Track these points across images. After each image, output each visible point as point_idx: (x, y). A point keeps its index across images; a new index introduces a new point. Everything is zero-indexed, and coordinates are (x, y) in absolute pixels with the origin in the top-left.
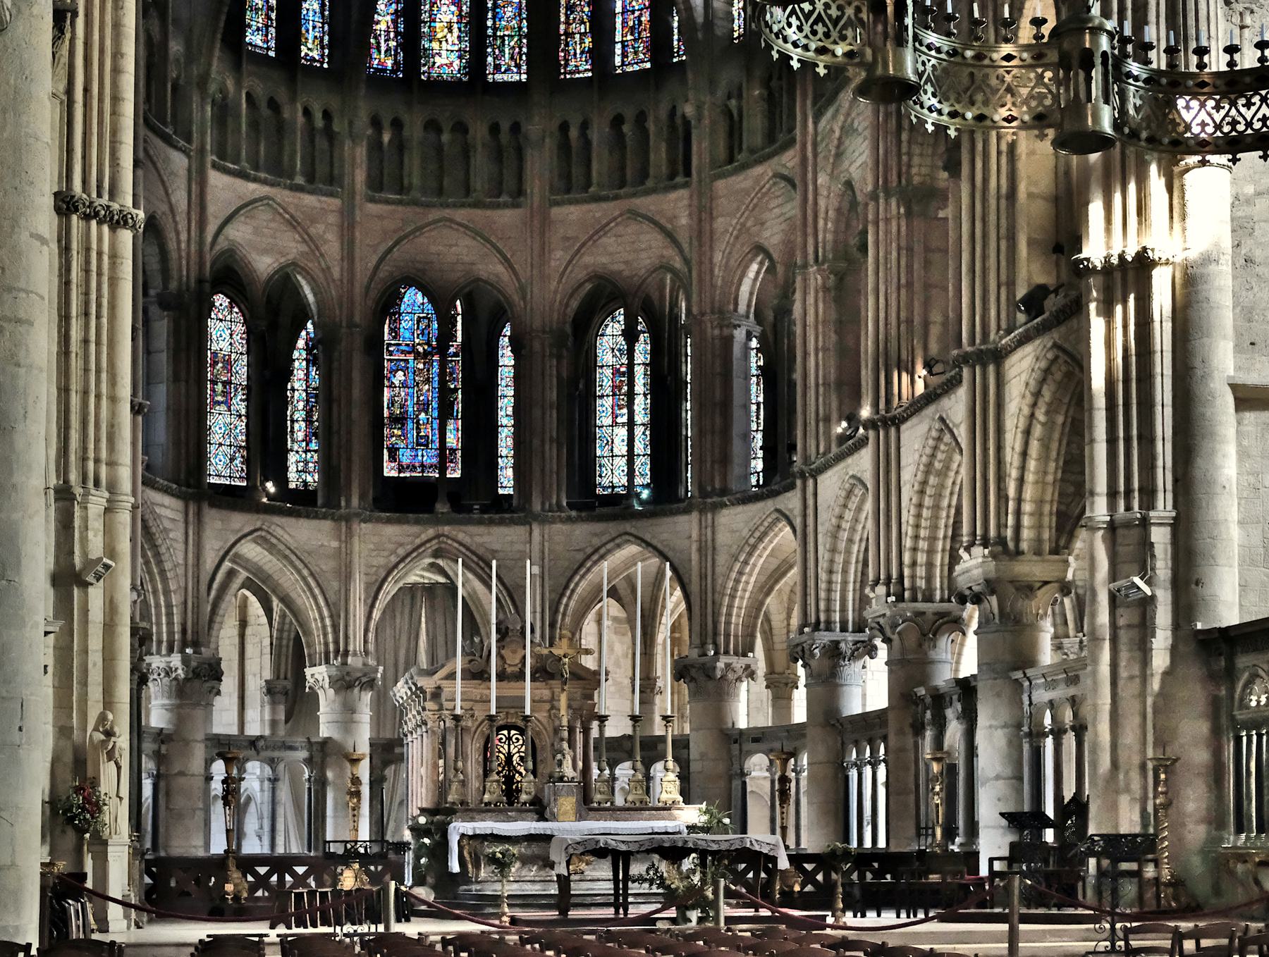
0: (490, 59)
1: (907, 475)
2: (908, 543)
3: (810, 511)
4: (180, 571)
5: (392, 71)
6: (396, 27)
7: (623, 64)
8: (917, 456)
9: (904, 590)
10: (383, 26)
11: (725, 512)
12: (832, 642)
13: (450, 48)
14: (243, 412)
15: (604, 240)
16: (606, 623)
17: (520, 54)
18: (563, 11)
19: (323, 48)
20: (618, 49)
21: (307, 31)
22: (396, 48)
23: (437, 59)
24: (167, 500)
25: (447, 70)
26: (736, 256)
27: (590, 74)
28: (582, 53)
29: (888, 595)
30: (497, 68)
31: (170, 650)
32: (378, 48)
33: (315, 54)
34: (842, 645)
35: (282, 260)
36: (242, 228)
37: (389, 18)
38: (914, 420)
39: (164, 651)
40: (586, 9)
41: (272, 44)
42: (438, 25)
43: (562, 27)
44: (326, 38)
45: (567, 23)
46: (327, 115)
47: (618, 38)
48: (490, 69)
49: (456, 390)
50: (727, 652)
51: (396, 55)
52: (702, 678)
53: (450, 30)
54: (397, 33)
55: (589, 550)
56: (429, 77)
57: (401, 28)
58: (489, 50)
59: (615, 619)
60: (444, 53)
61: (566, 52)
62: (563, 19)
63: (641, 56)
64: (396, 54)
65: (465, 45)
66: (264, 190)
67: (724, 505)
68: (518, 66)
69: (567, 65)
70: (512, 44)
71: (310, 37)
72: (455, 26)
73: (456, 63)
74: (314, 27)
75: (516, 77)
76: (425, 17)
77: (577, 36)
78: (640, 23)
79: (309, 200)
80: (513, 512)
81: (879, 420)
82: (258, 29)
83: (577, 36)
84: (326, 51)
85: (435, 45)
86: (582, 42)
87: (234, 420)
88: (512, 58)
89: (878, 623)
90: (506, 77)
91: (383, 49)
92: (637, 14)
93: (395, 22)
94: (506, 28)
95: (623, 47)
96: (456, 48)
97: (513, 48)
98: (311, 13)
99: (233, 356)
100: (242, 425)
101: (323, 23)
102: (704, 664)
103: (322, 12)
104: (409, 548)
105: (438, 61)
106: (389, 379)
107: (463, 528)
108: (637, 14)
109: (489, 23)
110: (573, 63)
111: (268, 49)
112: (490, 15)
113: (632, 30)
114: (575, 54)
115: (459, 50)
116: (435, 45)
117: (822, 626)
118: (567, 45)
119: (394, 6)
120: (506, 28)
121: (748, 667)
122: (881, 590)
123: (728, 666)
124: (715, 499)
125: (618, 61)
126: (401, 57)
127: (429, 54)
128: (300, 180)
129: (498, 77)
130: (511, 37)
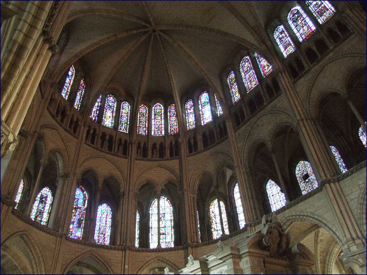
7: (154, 134)
19: (78, 107)
23: (106, 122)
28: (143, 131)
30: (121, 129)
35: (57, 147)
43: (138, 125)
44: (79, 106)
45: (139, 124)
47: (153, 129)
49: (83, 220)
54: (96, 113)
55: (145, 262)
60: (107, 121)
61: (139, 130)
62: (138, 123)
64: (95, 118)
77: (142, 128)
83: (142, 128)
84: (79, 109)
85: (106, 119)
86: (143, 129)
88: (125, 128)
90: (123, 131)
93: (97, 111)
105: (106, 123)
110: (140, 132)
113: (157, 128)
114: (141, 131)
116: (106, 119)
118: (139, 128)
126: (97, 118)
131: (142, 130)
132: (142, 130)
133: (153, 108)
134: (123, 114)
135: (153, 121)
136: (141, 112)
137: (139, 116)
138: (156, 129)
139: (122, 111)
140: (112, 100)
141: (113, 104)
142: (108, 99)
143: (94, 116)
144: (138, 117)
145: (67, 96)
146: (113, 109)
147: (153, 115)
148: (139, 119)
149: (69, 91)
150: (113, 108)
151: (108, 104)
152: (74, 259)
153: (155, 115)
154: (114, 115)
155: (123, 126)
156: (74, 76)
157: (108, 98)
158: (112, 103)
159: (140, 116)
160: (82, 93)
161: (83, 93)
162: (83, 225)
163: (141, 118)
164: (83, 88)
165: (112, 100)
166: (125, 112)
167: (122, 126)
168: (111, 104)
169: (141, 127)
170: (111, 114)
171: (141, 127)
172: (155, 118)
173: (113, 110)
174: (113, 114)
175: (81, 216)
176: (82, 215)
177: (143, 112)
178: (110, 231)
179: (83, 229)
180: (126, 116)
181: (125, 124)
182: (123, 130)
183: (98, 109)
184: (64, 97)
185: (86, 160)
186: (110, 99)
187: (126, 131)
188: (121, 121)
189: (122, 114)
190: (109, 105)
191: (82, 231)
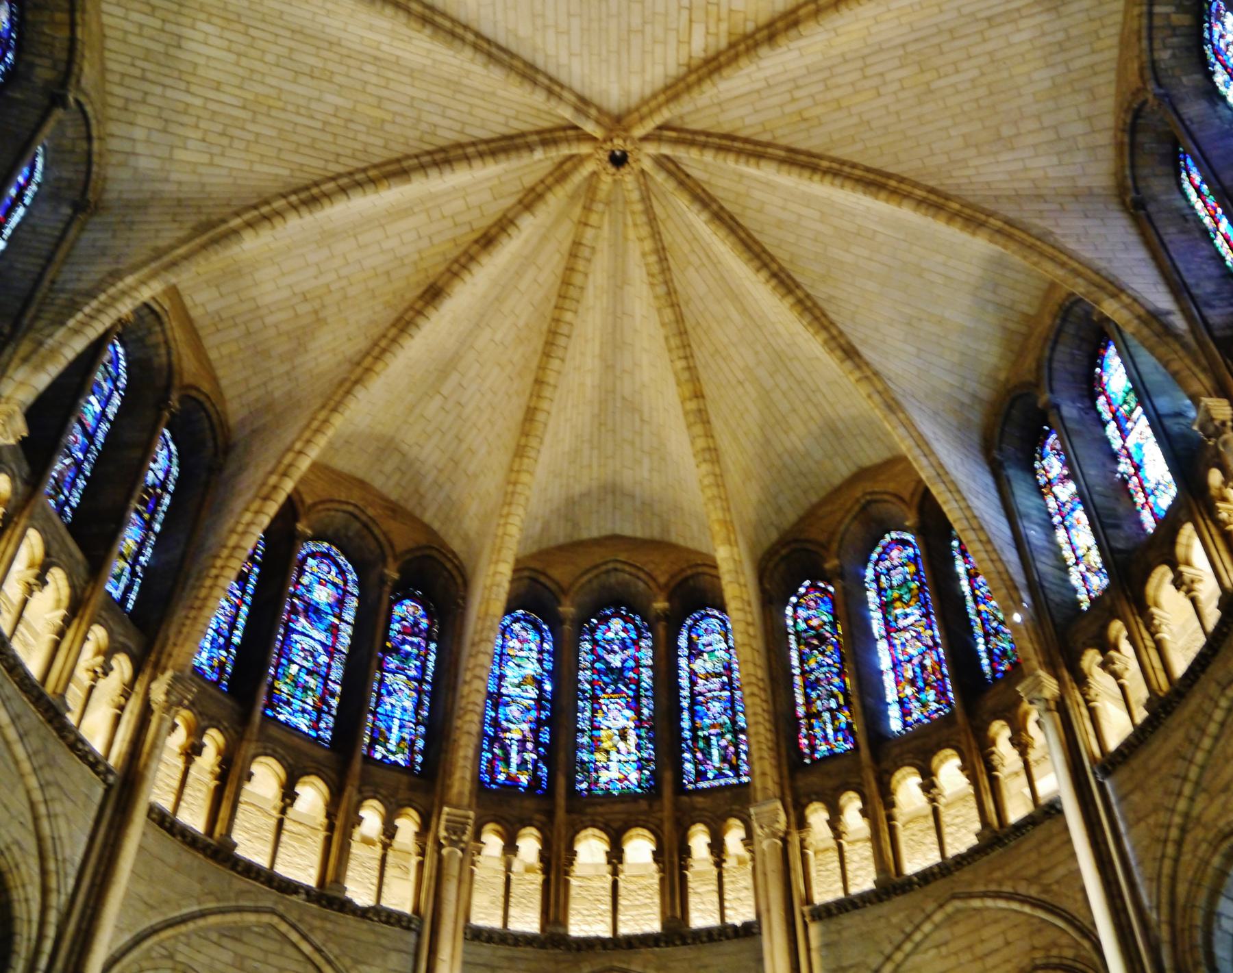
0: (688, 766)
7: (905, 724)
10: (517, 735)
13: (623, 758)
15: (916, 959)
17: (737, 754)
19: (412, 751)
20: (894, 712)
21: (389, 729)
22: (535, 763)
25: (619, 785)
26: (1186, 873)
28: (836, 731)
30: (701, 775)
36: (213, 951)
37: (525, 727)
42: (603, 733)
43: (801, 711)
44: (420, 744)
45: (809, 702)
47: (891, 695)
53: (623, 735)
54: (537, 744)
56: (589, 790)
57: (545, 737)
60: (614, 765)
61: (812, 738)
62: (800, 699)
64: (536, 768)
68: (735, 769)
70: (723, 743)
71: (394, 737)
73: (634, 776)
75: (735, 781)
82: (304, 711)
83: (826, 716)
84: (419, 759)
86: (834, 719)
88: (724, 759)
90: (716, 783)
91: (515, 759)
92: (916, 661)
93: (535, 732)
94: (713, 726)
96: (635, 758)
97: (726, 747)
98: (398, 713)
103: (416, 713)
105: (604, 776)
108: (916, 661)
109: (686, 724)
110: (823, 748)
112: (686, 715)
114: (825, 738)
115: (640, 760)
116: (600, 756)
118: (811, 727)
119: (534, 714)
120: (713, 726)
125: (895, 725)
127: (590, 770)
129: (703, 785)
130: (721, 735)
131: (830, 731)
132: (830, 731)
133: (870, 573)
134: (700, 682)
135: (882, 646)
137: (794, 655)
138: (909, 691)
139: (693, 673)
140: (623, 635)
141: (631, 651)
142: (599, 636)
143: (523, 762)
144: (795, 662)
145: (328, 721)
146: (638, 682)
148: (803, 673)
150: (631, 675)
151: (598, 665)
153: (885, 607)
154: (645, 711)
155: (715, 753)
156: (353, 603)
157: (593, 630)
158: (624, 647)
160: (423, 669)
161: (431, 665)
163: (813, 664)
164: (428, 639)
166: (709, 666)
167: (707, 755)
168: (616, 661)
169: (818, 715)
171: (818, 715)
172: (887, 623)
173: (637, 691)
174: (638, 712)
177: (814, 623)
180: (722, 689)
181: (721, 735)
182: (720, 774)
183: (543, 715)
184: (305, 729)
186: (610, 635)
187: (738, 775)
189: (693, 683)
190: (609, 669)
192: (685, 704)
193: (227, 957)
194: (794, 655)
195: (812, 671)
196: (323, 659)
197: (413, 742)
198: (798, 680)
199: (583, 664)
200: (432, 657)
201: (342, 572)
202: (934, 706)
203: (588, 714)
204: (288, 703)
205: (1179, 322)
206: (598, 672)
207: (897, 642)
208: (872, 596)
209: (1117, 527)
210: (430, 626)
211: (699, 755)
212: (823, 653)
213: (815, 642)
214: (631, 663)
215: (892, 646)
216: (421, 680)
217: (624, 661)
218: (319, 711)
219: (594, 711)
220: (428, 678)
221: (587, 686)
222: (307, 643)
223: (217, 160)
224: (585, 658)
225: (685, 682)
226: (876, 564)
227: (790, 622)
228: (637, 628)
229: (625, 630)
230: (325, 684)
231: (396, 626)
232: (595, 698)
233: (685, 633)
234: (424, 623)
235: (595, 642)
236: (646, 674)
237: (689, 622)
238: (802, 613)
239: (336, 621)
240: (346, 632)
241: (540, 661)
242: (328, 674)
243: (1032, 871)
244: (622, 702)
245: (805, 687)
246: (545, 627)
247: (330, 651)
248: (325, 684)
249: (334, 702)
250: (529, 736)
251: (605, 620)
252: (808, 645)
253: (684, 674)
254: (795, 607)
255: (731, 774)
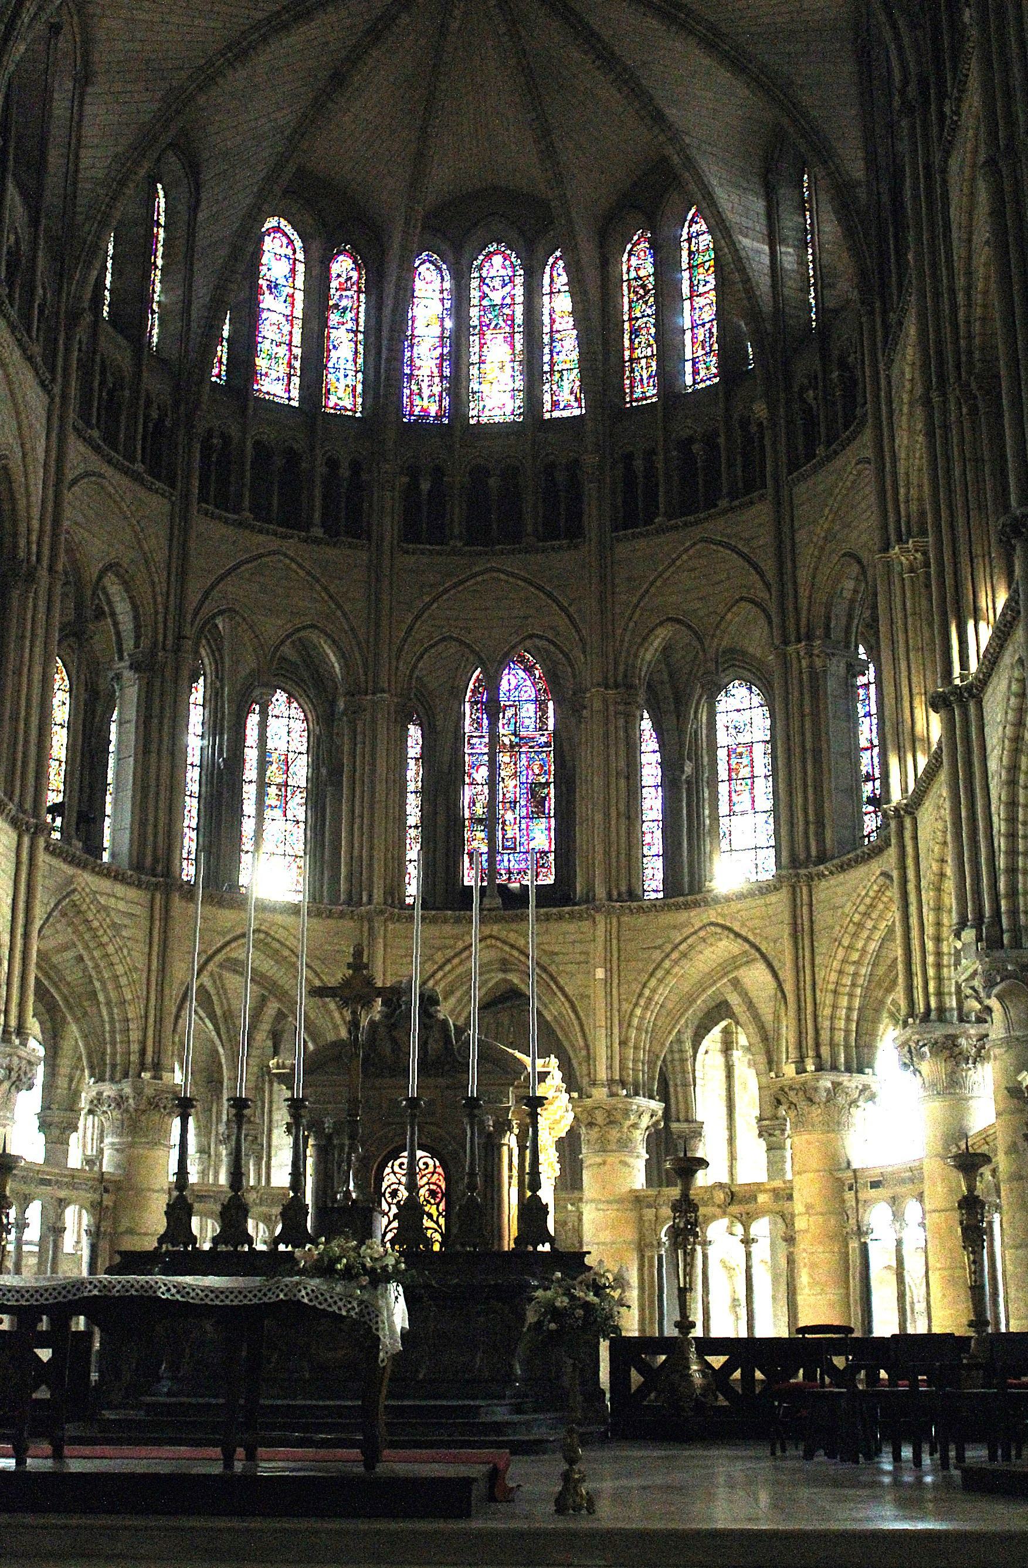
0: (547, 397)
1: (993, 765)
2: (1002, 862)
3: (910, 862)
4: (140, 977)
5: (436, 417)
6: (441, 371)
7: (695, 383)
8: (1001, 728)
9: (1002, 932)
11: (824, 884)
12: (947, 1037)
14: (302, 818)
16: (737, 1055)
18: (626, 336)
20: (688, 366)
24: (132, 893)
27: (654, 400)
29: (979, 939)
30: (555, 405)
31: (126, 1075)
32: (420, 394)
33: (347, 403)
34: (963, 1041)
37: (434, 363)
38: (994, 680)
39: (118, 1076)
40: (653, 331)
41: (295, 393)
43: (627, 353)
44: (359, 388)
45: (632, 349)
46: (356, 467)
47: (688, 355)
48: (548, 406)
50: (834, 1068)
51: (440, 401)
52: (802, 1104)
57: (447, 372)
58: (546, 387)
59: (748, 1049)
61: (632, 379)
62: (627, 343)
63: (715, 371)
65: (519, 384)
66: (275, 544)
67: (821, 876)
69: (632, 393)
72: (508, 366)
74: (346, 376)
76: (475, 359)
78: (711, 333)
79: (331, 553)
80: (575, 904)
81: (952, 693)
83: (643, 362)
84: (359, 400)
87: (290, 825)
89: (973, 988)
90: (566, 414)
91: (426, 393)
92: (708, 326)
93: (440, 367)
95: (694, 364)
99: (291, 756)
100: (299, 832)
101: (357, 372)
102: (804, 1083)
104: (450, 953)
106: (470, 776)
107: (514, 926)
108: (708, 326)
109: (546, 358)
111: (289, 399)
112: (546, 350)
114: (641, 380)
117: (933, 1015)
118: (632, 371)
119: (439, 350)
121: (865, 1088)
122: (968, 935)
123: (836, 1085)
124: (814, 870)
125: (689, 380)
126: (446, 403)
128: (318, 532)
129: (556, 414)
131: (645, 377)
133: (686, 230)
135: (687, 304)
136: (633, 274)
137: (626, 300)
138: (701, 352)
139: (552, 311)
141: (508, 288)
144: (626, 308)
147: (686, 275)
148: (630, 319)
149: (298, 351)
150: (506, 311)
152: (433, 975)
156: (301, 268)
157: (480, 268)
159: (631, 302)
161: (362, 315)
162: (551, 804)
165: (503, 272)
170: (507, 348)
172: (691, 286)
173: (512, 326)
174: (513, 347)
175: (537, 771)
176: (542, 767)
178: (658, 804)
179: (553, 821)
183: (446, 351)
185: (417, 618)
188: (552, 365)
189: (553, 321)
191: (549, 829)
192: (546, 339)
193: (256, 587)
194: (626, 300)
195: (637, 319)
196: (286, 328)
197: (354, 388)
198: (627, 326)
199: (475, 301)
200: (362, 309)
201: (291, 242)
202: (715, 371)
203: (477, 349)
204: (266, 375)
205: (862, 193)
206: (483, 309)
207: (696, 306)
208: (685, 254)
209: (832, 286)
210: (360, 278)
211: (555, 387)
212: (646, 303)
213: (641, 292)
214: (508, 301)
215: (693, 309)
216: (356, 332)
217: (504, 298)
218: (289, 376)
219: (481, 346)
220: (361, 329)
221: (477, 323)
222: (274, 318)
223: (167, 18)
224: (475, 294)
225: (546, 319)
226: (690, 226)
227: (625, 268)
228: (513, 266)
229: (504, 268)
230: (290, 350)
231: (334, 284)
232: (482, 334)
233: (548, 269)
234: (355, 275)
235: (482, 279)
236: (519, 310)
237: (551, 260)
238: (634, 261)
239: (291, 291)
240: (299, 296)
241: (442, 300)
242: (291, 341)
243: (745, 535)
244: (501, 337)
245: (631, 333)
246: (444, 266)
247: (290, 319)
248: (290, 350)
249: (297, 364)
250: (436, 371)
251: (489, 256)
252: (636, 293)
253: (546, 311)
254: (630, 254)
255: (576, 405)
